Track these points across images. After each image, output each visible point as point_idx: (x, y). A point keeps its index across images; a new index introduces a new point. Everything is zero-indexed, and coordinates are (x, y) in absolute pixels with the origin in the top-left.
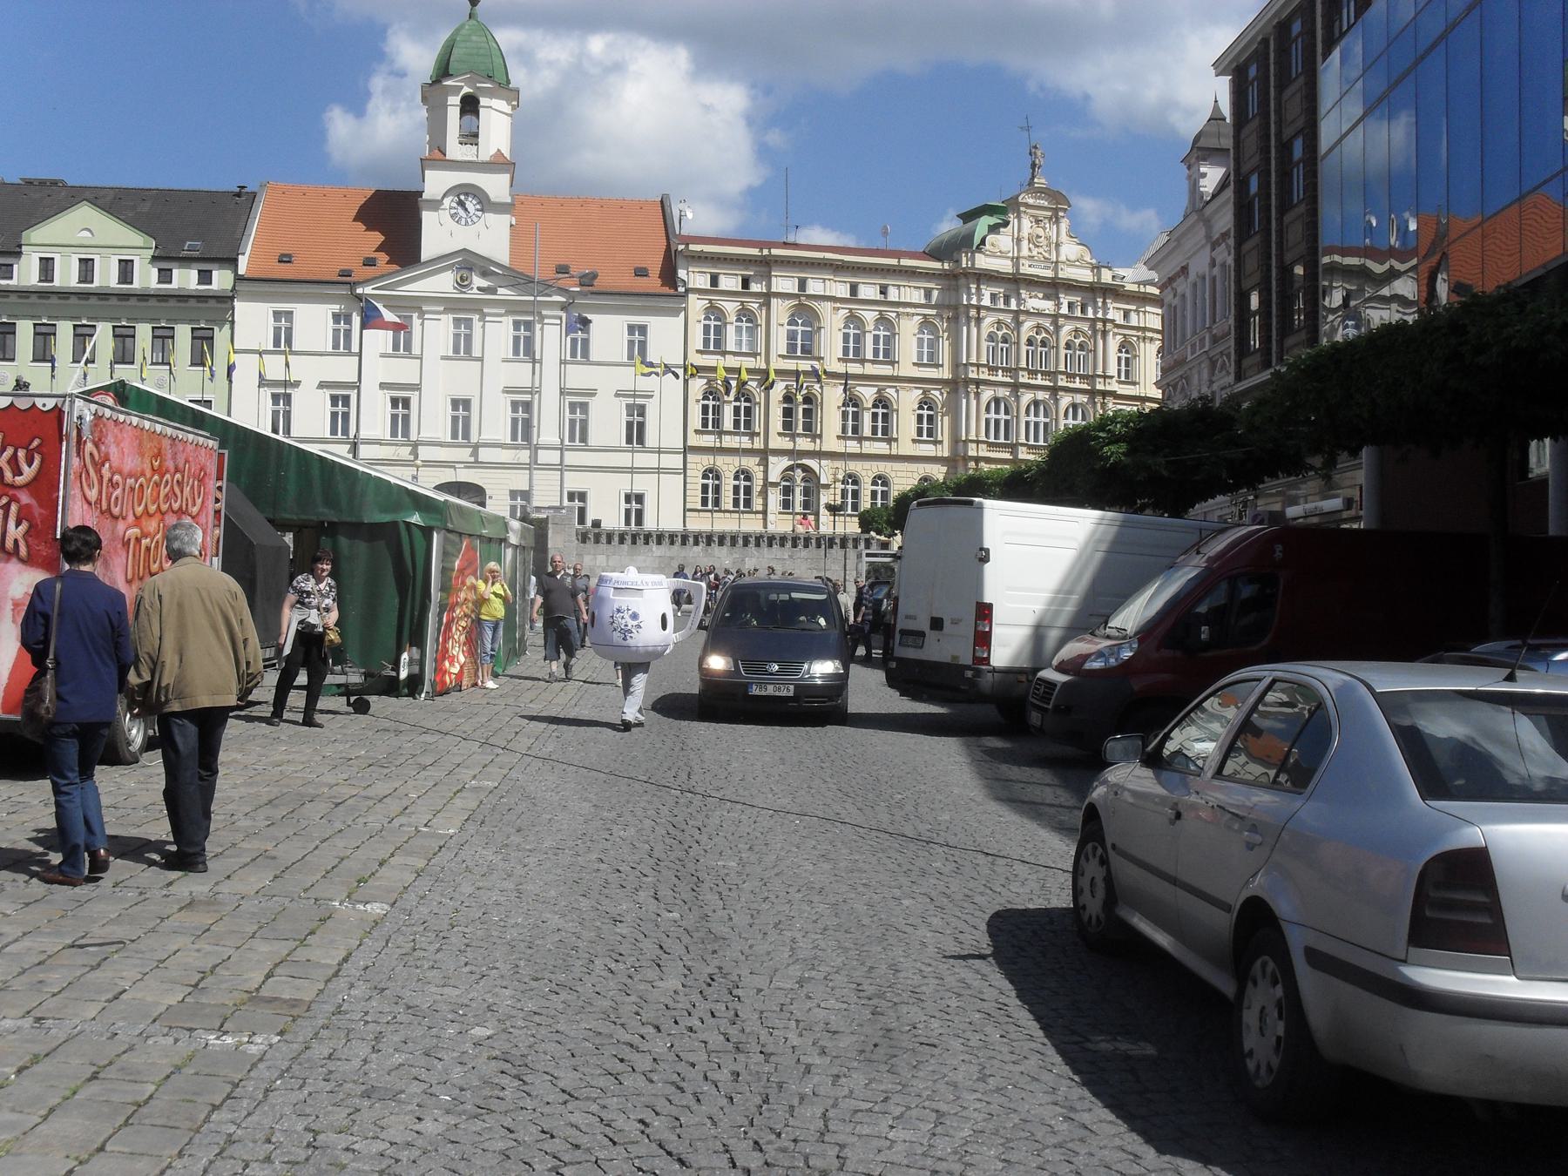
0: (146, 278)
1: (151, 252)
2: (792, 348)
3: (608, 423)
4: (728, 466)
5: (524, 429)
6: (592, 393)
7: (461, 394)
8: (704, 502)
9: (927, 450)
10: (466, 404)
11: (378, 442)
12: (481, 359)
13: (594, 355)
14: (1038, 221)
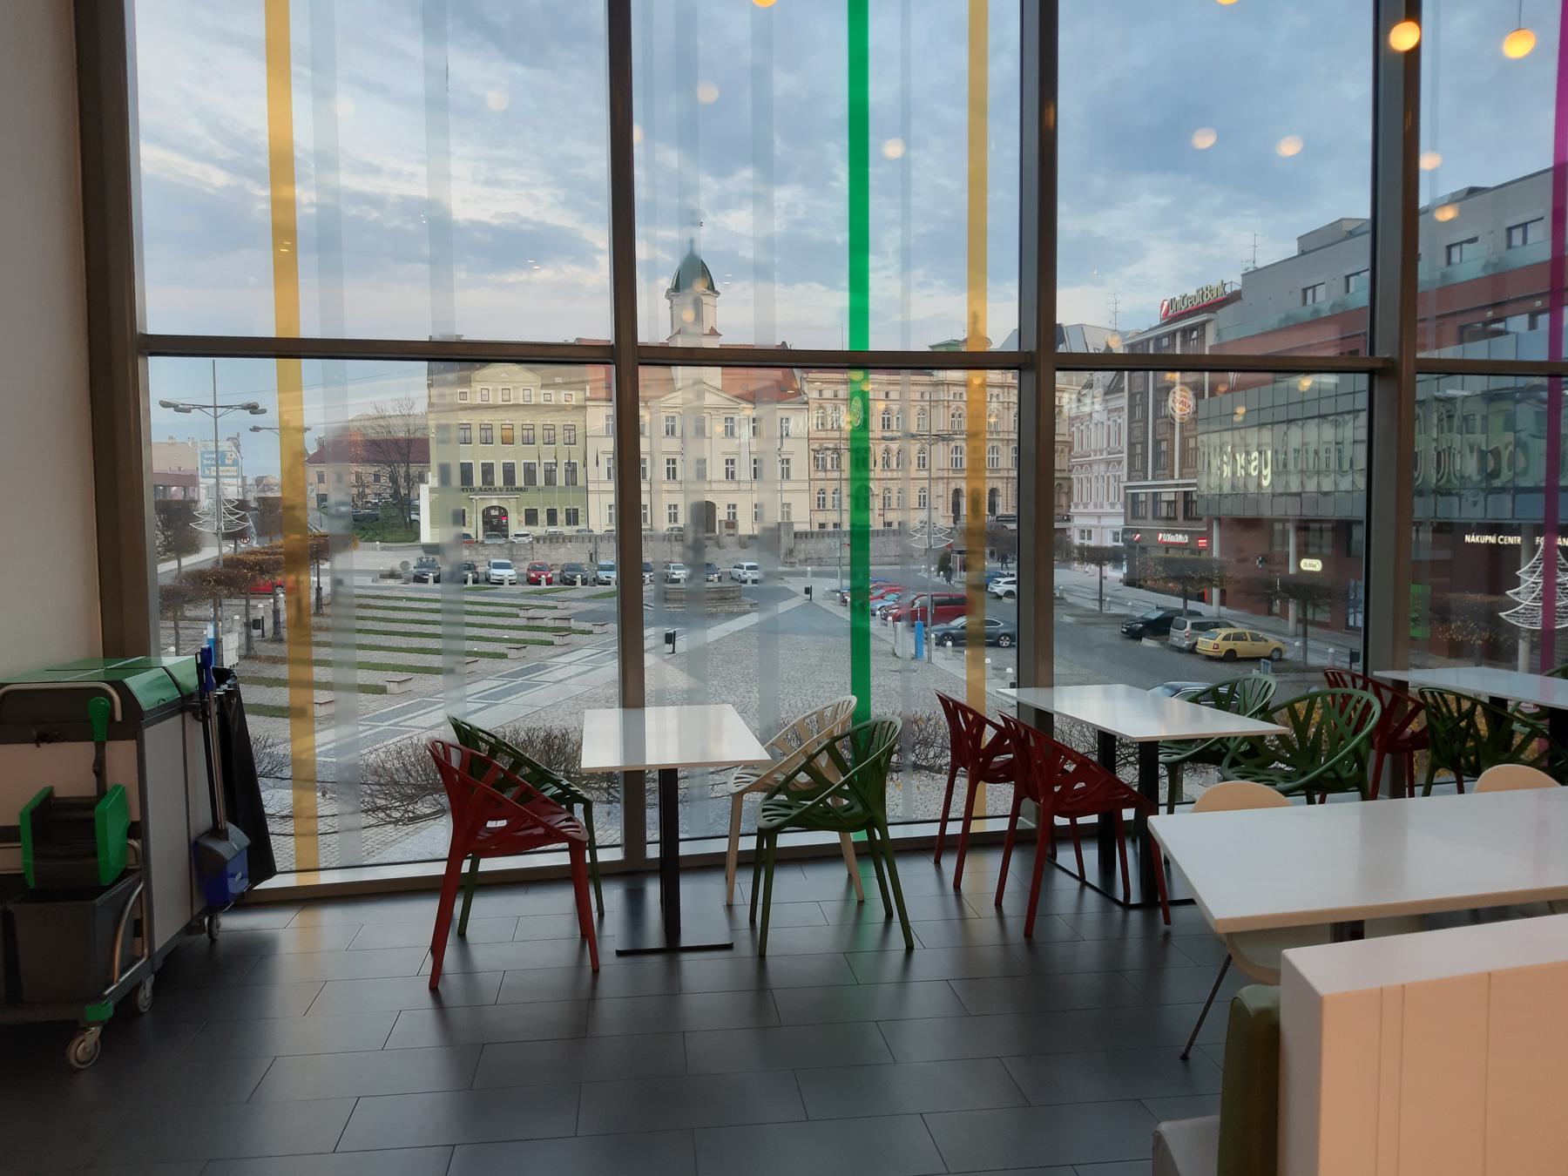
0: (538, 397)
5: (730, 475)
8: (819, 505)
12: (711, 438)
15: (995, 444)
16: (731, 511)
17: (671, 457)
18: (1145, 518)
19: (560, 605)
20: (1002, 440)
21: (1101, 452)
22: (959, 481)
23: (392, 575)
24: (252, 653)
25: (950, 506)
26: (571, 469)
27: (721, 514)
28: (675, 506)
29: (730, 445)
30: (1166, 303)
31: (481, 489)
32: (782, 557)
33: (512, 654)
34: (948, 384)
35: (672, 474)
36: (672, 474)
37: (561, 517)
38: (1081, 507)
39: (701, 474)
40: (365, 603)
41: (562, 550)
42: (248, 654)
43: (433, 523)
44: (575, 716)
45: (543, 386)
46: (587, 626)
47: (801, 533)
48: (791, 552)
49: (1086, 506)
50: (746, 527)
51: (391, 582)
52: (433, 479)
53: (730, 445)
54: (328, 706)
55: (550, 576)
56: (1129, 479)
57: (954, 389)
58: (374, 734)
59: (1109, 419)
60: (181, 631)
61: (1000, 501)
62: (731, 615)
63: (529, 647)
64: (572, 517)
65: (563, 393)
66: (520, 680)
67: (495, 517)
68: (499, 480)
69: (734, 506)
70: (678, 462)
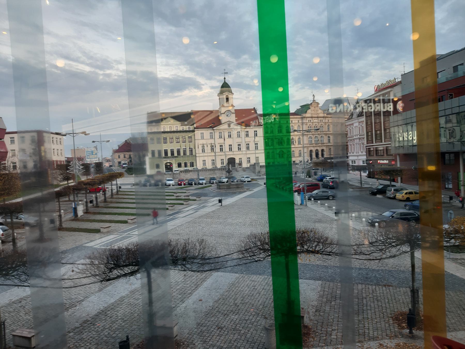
0: (180, 128)
1: (180, 125)
2: (279, 132)
3: (252, 146)
4: (271, 151)
5: (239, 149)
6: (250, 142)
7: (230, 144)
9: (300, 146)
10: (231, 145)
11: (219, 152)
13: (249, 136)
14: (315, 107)
15: (322, 135)
16: (240, 160)
17: (221, 144)
18: (373, 156)
19: (187, 192)
20: (324, 134)
21: (357, 135)
22: (311, 148)
23: (136, 184)
24: (88, 211)
25: (309, 155)
26: (191, 151)
27: (237, 161)
28: (223, 160)
29: (239, 140)
30: (376, 87)
31: (164, 157)
32: (257, 174)
33: (170, 208)
34: (306, 118)
35: (221, 150)
36: (221, 150)
37: (189, 164)
38: (352, 153)
39: (231, 149)
40: (126, 193)
41: (189, 175)
42: (86, 212)
43: (151, 168)
44: (188, 229)
45: (181, 126)
46: (195, 198)
47: (262, 166)
48: (259, 172)
49: (353, 153)
50: (245, 165)
51: (136, 187)
52: (150, 155)
53: (239, 140)
54: (107, 228)
55: (185, 183)
56: (367, 144)
57: (308, 119)
58: (121, 238)
59: (359, 125)
60: (61, 205)
61: (325, 153)
62: (240, 193)
63: (176, 206)
64: (192, 165)
65: (188, 127)
66: (171, 217)
67: (169, 165)
68: (169, 155)
69: (241, 159)
70: (223, 146)
